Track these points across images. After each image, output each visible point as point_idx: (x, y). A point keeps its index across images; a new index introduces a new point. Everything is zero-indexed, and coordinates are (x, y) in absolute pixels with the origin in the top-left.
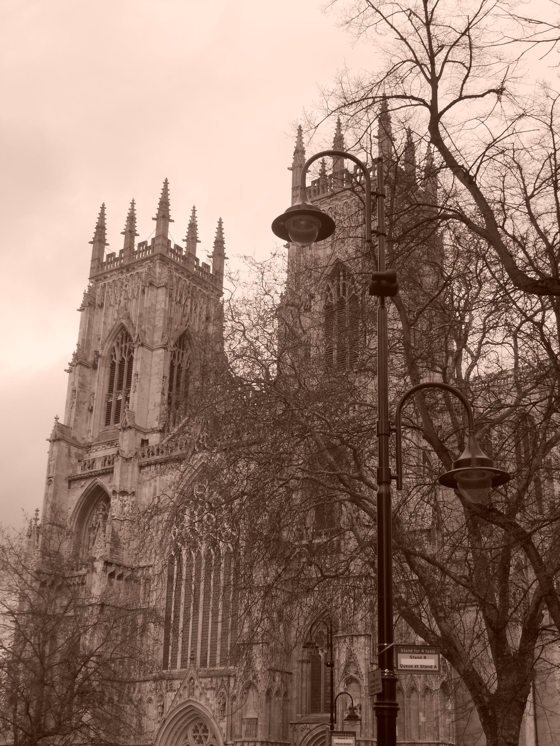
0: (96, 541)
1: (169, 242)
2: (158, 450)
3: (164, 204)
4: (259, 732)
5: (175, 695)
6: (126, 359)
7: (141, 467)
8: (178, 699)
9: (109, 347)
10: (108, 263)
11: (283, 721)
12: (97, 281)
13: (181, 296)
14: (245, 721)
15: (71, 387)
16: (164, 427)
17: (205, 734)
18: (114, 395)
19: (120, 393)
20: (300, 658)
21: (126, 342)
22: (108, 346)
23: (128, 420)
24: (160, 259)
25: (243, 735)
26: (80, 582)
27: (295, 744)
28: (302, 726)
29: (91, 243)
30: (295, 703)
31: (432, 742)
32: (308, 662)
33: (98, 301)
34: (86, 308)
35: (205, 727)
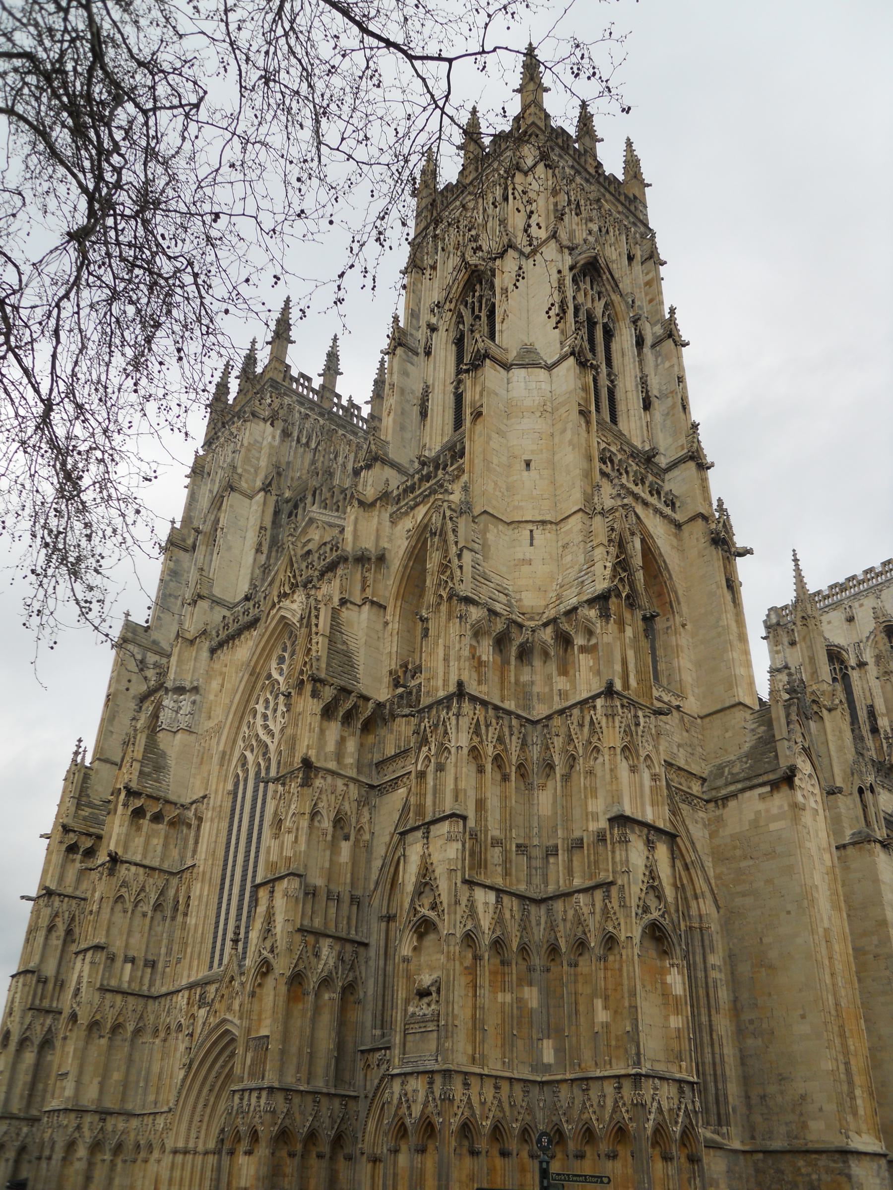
1: (288, 367)
7: (213, 651)
8: (212, 1019)
11: (340, 1046)
20: (384, 912)
24: (271, 386)
27: (366, 1097)
28: (378, 1055)
30: (370, 1006)
31: (623, 1072)
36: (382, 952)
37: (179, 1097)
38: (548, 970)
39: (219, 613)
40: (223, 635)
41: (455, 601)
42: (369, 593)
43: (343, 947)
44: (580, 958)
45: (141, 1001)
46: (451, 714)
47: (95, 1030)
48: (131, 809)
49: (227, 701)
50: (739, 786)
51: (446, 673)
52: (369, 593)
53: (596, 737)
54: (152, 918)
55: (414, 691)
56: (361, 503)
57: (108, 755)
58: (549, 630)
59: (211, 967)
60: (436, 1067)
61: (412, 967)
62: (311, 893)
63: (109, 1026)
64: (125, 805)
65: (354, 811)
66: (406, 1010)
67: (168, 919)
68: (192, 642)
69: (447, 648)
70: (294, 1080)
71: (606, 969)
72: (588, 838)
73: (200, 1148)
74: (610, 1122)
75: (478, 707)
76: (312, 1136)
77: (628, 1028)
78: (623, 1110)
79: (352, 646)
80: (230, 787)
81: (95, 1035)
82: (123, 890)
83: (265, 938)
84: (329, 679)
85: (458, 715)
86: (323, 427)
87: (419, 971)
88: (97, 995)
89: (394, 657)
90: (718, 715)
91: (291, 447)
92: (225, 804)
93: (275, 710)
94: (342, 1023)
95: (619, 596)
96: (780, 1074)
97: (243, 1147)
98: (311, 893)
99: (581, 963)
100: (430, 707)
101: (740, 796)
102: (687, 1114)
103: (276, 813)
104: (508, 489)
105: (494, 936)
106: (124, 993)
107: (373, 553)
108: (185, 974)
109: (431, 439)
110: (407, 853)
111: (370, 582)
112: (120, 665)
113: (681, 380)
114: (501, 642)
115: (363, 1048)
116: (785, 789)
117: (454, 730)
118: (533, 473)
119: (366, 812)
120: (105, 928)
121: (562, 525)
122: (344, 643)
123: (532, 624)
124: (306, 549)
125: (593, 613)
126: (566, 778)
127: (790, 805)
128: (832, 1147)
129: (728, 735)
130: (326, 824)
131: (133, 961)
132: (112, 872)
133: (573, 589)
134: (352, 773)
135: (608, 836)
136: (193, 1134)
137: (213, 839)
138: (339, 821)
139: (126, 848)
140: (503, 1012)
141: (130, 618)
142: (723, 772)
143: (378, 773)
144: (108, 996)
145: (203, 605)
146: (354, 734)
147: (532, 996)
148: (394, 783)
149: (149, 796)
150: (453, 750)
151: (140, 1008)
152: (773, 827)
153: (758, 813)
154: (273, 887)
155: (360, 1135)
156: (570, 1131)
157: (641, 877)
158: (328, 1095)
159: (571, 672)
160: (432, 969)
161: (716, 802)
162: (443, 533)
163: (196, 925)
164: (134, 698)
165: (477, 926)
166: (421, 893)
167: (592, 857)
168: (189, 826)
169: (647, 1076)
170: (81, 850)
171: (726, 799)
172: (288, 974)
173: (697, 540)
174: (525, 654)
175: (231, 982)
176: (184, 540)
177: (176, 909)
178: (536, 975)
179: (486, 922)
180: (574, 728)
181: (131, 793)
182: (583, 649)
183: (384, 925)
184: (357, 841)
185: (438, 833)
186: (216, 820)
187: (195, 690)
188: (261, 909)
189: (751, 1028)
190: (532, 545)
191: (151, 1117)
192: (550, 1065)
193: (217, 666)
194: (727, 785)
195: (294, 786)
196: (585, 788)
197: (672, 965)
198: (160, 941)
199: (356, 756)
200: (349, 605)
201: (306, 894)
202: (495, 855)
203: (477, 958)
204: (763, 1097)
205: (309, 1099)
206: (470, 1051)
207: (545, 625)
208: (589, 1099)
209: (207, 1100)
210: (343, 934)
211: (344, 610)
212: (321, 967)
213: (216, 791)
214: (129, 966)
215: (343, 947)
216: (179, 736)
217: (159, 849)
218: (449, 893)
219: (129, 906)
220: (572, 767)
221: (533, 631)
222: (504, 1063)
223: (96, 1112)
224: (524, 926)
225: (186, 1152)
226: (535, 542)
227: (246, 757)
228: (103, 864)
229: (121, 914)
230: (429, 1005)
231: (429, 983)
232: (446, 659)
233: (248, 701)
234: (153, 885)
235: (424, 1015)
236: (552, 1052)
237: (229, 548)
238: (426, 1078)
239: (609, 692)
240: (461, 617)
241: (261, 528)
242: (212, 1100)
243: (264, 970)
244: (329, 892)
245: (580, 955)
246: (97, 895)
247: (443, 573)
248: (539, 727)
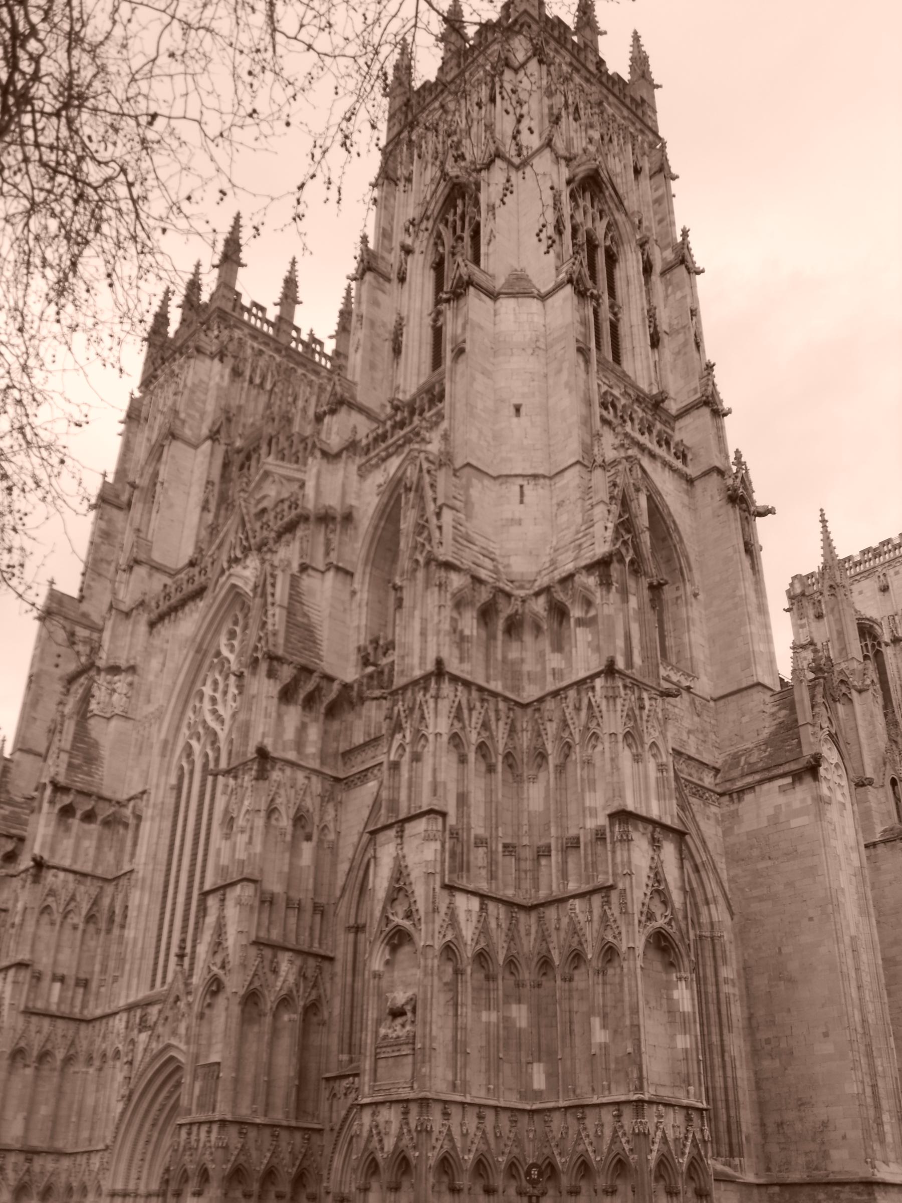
1: (239, 295)
5: (151, 1036)
7: (152, 625)
8: (154, 1045)
11: (302, 1074)
13: (264, 378)
20: (352, 922)
24: (219, 317)
25: (194, 1107)
27: (332, 1130)
28: (345, 1083)
30: (336, 1028)
31: (623, 1098)
36: (350, 966)
37: (117, 1133)
38: (539, 985)
39: (158, 582)
40: (164, 607)
41: (433, 566)
42: (333, 557)
43: (305, 962)
44: (576, 972)
45: (72, 1026)
46: (428, 696)
47: (19, 1059)
48: (58, 806)
49: (169, 682)
50: (757, 777)
51: (423, 650)
52: (333, 557)
53: (594, 723)
54: (84, 931)
55: (386, 670)
56: (325, 454)
57: (31, 745)
58: (542, 600)
59: (153, 986)
60: (412, 1096)
61: (384, 983)
62: (267, 901)
63: (35, 1053)
64: (52, 802)
65: (317, 809)
67: (103, 933)
68: (127, 615)
69: (424, 621)
70: (249, 1112)
71: (604, 983)
72: (585, 836)
73: (142, 1190)
74: (609, 1153)
75: (460, 688)
76: (270, 1174)
77: (630, 1050)
78: (623, 1140)
79: (315, 618)
80: (173, 781)
81: (19, 1063)
82: (50, 900)
83: (215, 953)
84: (288, 656)
85: (436, 698)
86: (279, 365)
87: (392, 988)
88: (21, 1021)
89: (363, 630)
90: (734, 697)
91: (242, 388)
92: (167, 800)
93: (225, 693)
94: (303, 1048)
95: (621, 560)
96: (799, 1099)
97: (191, 1187)
98: (267, 901)
99: (576, 978)
100: (404, 688)
101: (757, 788)
102: (695, 1144)
103: (226, 811)
104: (495, 438)
105: (478, 947)
106: (53, 1017)
107: (339, 511)
108: (124, 993)
109: (405, 380)
110: (378, 855)
111: (335, 544)
112: (44, 642)
113: (694, 313)
114: (486, 614)
115: (328, 1075)
116: (808, 780)
117: (432, 715)
118: (524, 419)
119: (330, 808)
120: (29, 942)
121: (557, 479)
122: (305, 615)
123: (522, 593)
124: (261, 506)
125: (591, 581)
126: (561, 769)
127: (813, 798)
128: (856, 1178)
129: (745, 719)
130: (285, 822)
131: (62, 979)
132: (36, 879)
133: (570, 553)
134: (315, 764)
135: (608, 835)
136: (134, 1175)
137: (154, 840)
138: (299, 819)
139: (53, 850)
140: (488, 1033)
141: (55, 587)
142: (739, 762)
143: (345, 764)
144: (34, 1019)
145: (141, 571)
146: (316, 720)
147: (520, 1015)
148: (363, 776)
149: (80, 792)
150: (431, 738)
151: (71, 1033)
152: (795, 823)
153: (778, 808)
154: (224, 895)
155: (325, 1173)
156: (563, 1164)
157: (645, 880)
158: (289, 1128)
159: (567, 648)
160: (407, 985)
161: (731, 795)
162: (419, 489)
163: (135, 939)
164: (61, 679)
165: (459, 936)
166: (394, 900)
167: (590, 859)
168: (126, 825)
169: (650, 1102)
171: (741, 792)
172: (242, 992)
173: (712, 497)
174: (513, 627)
176: (117, 496)
177: (111, 920)
178: (525, 991)
179: (468, 931)
180: (570, 712)
181: (58, 788)
182: (580, 622)
183: (351, 936)
184: (320, 842)
185: (414, 832)
186: (158, 819)
187: (132, 669)
188: (211, 919)
189: (768, 1047)
190: (522, 502)
191: (85, 1156)
192: (541, 1092)
193: (157, 642)
194: (743, 776)
195: (247, 779)
196: (582, 780)
197: (680, 979)
198: (94, 957)
199: (319, 745)
200: (310, 572)
201: (262, 902)
202: (479, 856)
203: (458, 972)
204: (780, 1125)
205: (267, 1132)
206: (450, 1077)
207: (537, 594)
208: (585, 1129)
209: (150, 1136)
210: (305, 948)
211: (304, 576)
212: (279, 984)
213: (157, 786)
214: (57, 986)
215: (305, 962)
216: (114, 723)
217: (92, 852)
218: (427, 899)
219: (58, 918)
220: (567, 756)
221: (524, 601)
222: (489, 1089)
223: (21, 1151)
224: (512, 938)
226: (526, 499)
227: (190, 747)
228: (27, 870)
229: (48, 927)
230: (403, 1026)
231: (403, 1001)
232: (423, 634)
233: (193, 682)
234: (85, 893)
235: (398, 1037)
236: (543, 1077)
237: (171, 506)
238: (400, 1108)
239: (610, 670)
240: (440, 585)
241: (208, 482)
242: (155, 1135)
243: (214, 988)
244: (289, 900)
245: (576, 968)
246: (20, 906)
247: (420, 534)
248: (530, 711)
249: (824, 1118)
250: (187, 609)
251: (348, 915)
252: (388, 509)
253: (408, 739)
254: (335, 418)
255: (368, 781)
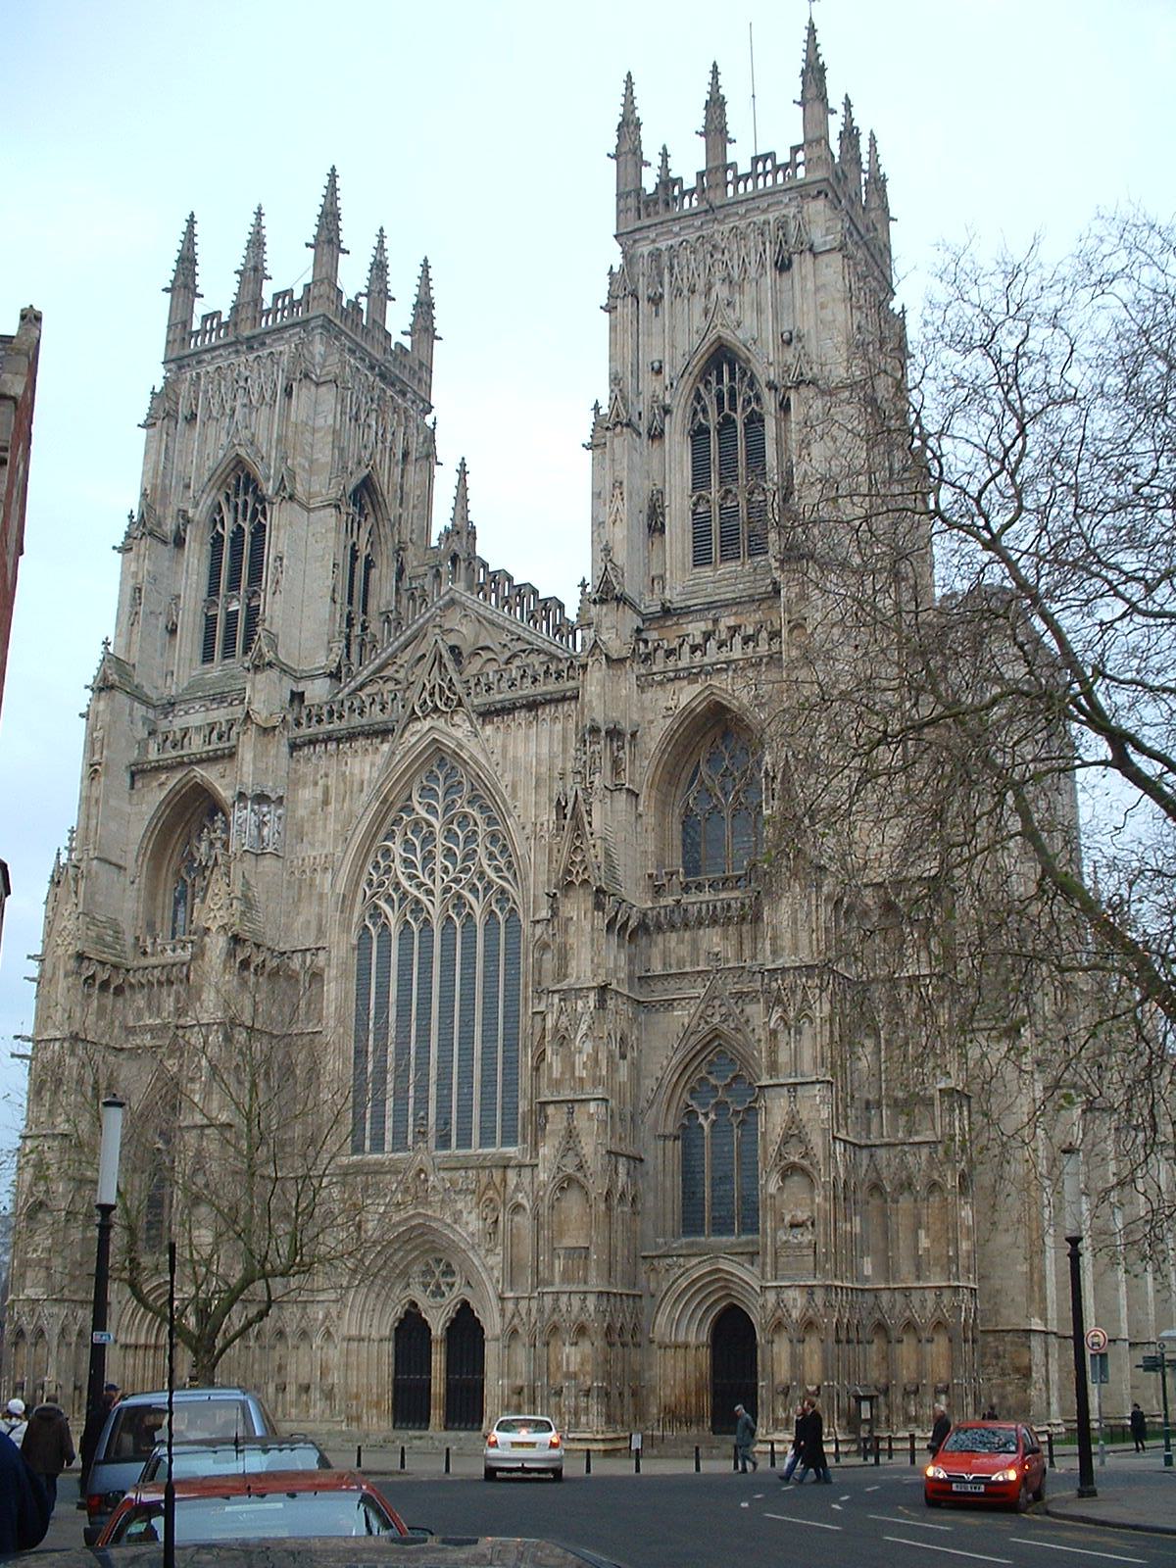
0: (210, 893)
1: (340, 292)
2: (331, 713)
3: (330, 217)
4: (593, 1273)
6: (247, 527)
7: (294, 747)
9: (209, 502)
10: (203, 332)
12: (180, 368)
14: (562, 1252)
15: (131, 582)
16: (339, 667)
17: (449, 1280)
18: (221, 601)
19: (233, 597)
20: (660, 1131)
21: (246, 494)
22: (206, 502)
23: (265, 650)
24: (322, 326)
25: (557, 1280)
26: (163, 979)
27: (653, 1296)
28: (669, 1261)
29: (166, 290)
31: (944, 1284)
32: (676, 1138)
33: (183, 410)
34: (159, 423)
35: (449, 1265)
36: (661, 1168)
52: (625, 779)
59: (358, 1149)
66: (774, 1239)
92: (350, 961)
93: (429, 857)
115: (646, 1254)
135: (937, 1102)
143: (641, 987)
158: (627, 1295)
165: (838, 1172)
170: (97, 982)
175: (418, 1175)
197: (966, 1203)
225: (361, 1339)
227: (376, 907)
231: (805, 1218)
233: (375, 836)
236: (870, 1267)
249: (998, 1287)
250: (357, 745)
251: (656, 1121)
252: (677, 736)
253: (792, 1014)
254: (605, 608)
255: (673, 1009)
